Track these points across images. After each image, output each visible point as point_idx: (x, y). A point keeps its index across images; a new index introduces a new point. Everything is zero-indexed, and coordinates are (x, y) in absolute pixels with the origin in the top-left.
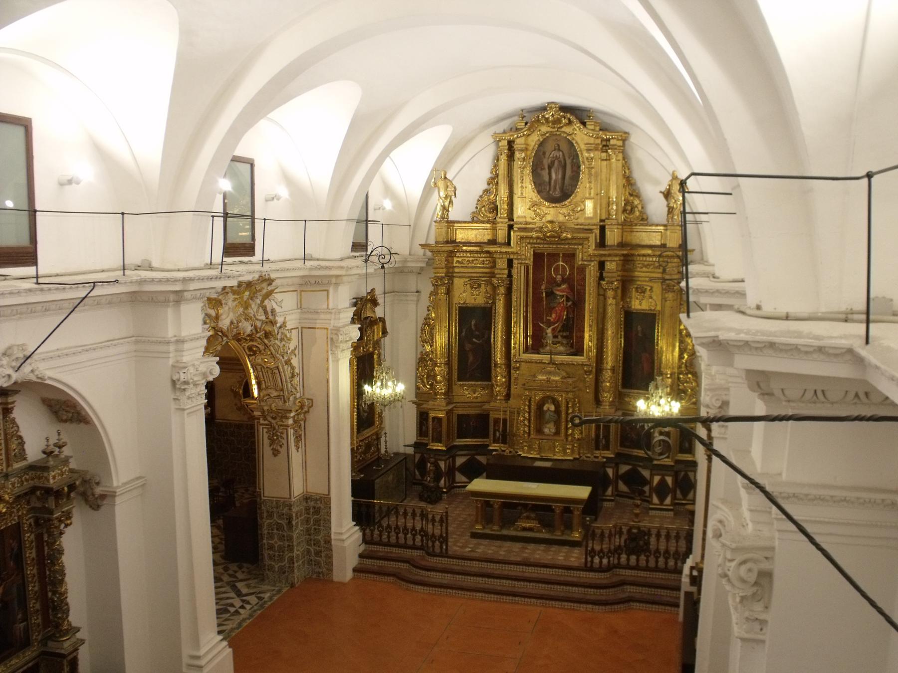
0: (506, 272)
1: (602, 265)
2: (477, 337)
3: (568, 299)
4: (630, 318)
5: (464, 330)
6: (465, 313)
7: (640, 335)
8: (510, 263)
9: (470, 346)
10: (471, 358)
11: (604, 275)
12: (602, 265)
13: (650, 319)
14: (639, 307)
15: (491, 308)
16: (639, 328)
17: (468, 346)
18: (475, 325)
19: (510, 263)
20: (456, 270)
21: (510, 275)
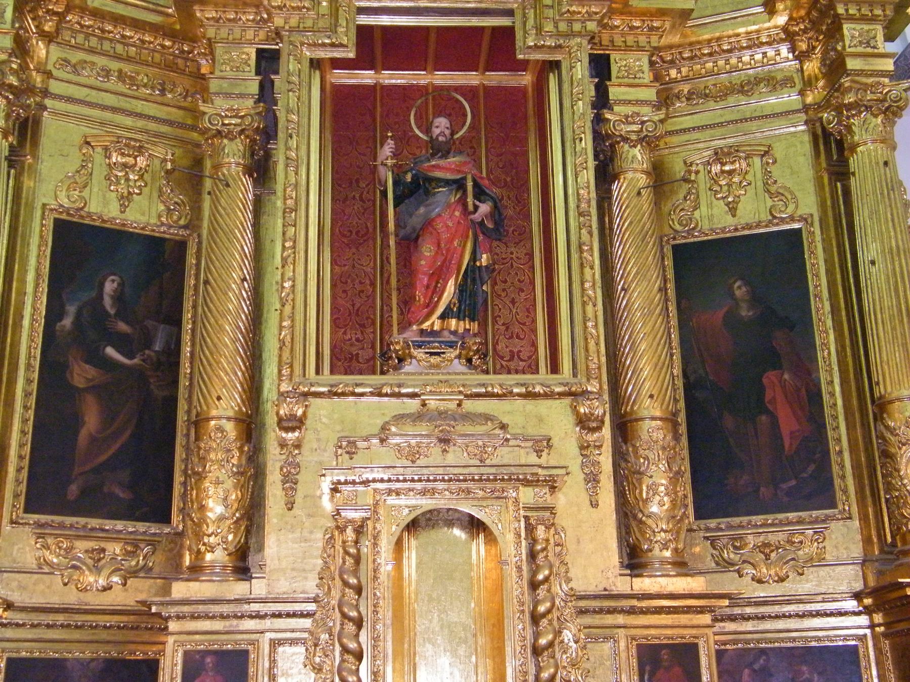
0: (253, 87)
1: (600, 67)
2: (124, 344)
3: (480, 194)
4: (696, 265)
5: (71, 309)
6: (79, 246)
7: (745, 312)
8: (268, 61)
9: (91, 372)
10: (91, 420)
11: (615, 92)
12: (600, 67)
13: (773, 257)
14: (729, 221)
15: (182, 246)
16: (740, 290)
17: (82, 374)
18: (118, 298)
19: (268, 61)
20: (55, 87)
21: (266, 93)
